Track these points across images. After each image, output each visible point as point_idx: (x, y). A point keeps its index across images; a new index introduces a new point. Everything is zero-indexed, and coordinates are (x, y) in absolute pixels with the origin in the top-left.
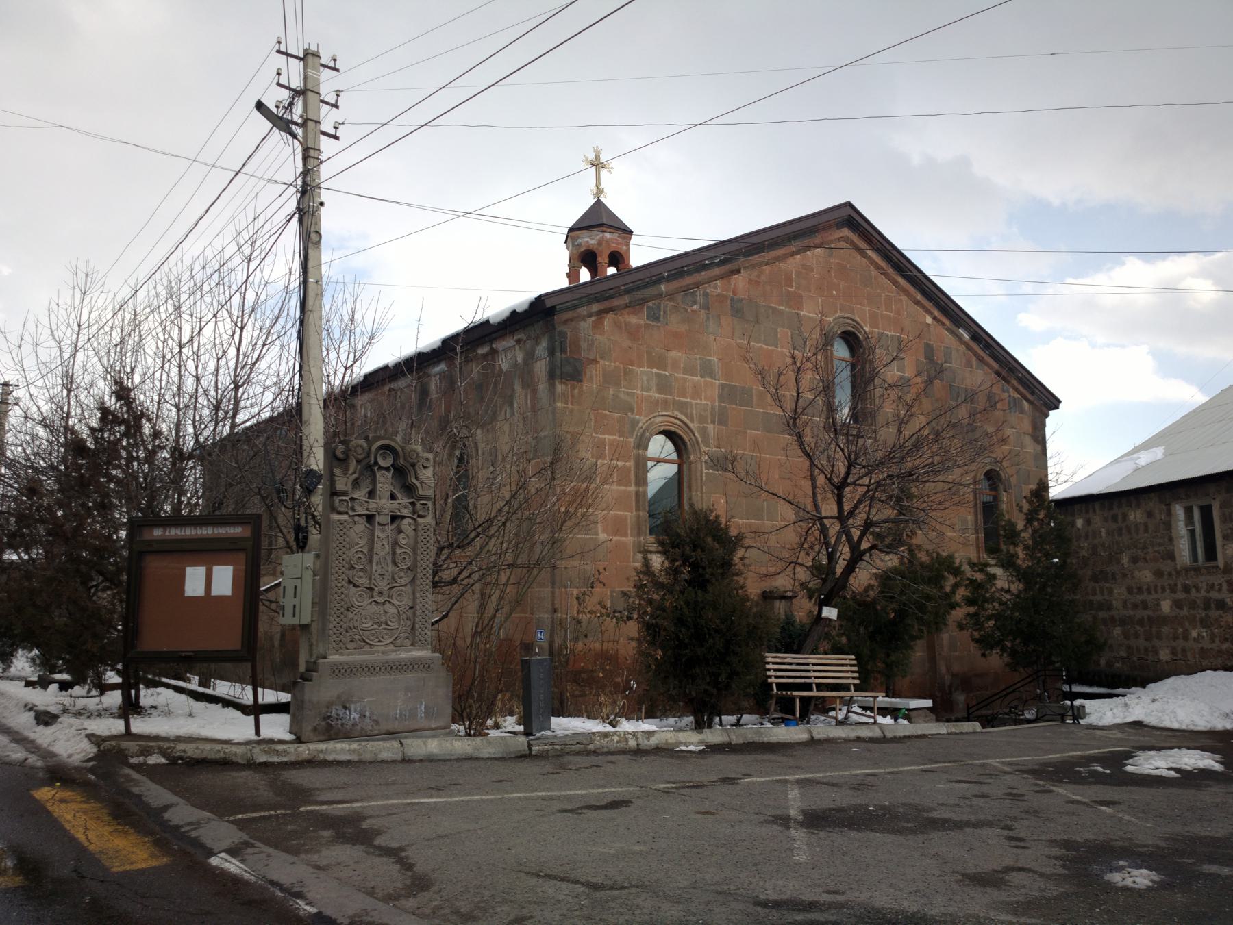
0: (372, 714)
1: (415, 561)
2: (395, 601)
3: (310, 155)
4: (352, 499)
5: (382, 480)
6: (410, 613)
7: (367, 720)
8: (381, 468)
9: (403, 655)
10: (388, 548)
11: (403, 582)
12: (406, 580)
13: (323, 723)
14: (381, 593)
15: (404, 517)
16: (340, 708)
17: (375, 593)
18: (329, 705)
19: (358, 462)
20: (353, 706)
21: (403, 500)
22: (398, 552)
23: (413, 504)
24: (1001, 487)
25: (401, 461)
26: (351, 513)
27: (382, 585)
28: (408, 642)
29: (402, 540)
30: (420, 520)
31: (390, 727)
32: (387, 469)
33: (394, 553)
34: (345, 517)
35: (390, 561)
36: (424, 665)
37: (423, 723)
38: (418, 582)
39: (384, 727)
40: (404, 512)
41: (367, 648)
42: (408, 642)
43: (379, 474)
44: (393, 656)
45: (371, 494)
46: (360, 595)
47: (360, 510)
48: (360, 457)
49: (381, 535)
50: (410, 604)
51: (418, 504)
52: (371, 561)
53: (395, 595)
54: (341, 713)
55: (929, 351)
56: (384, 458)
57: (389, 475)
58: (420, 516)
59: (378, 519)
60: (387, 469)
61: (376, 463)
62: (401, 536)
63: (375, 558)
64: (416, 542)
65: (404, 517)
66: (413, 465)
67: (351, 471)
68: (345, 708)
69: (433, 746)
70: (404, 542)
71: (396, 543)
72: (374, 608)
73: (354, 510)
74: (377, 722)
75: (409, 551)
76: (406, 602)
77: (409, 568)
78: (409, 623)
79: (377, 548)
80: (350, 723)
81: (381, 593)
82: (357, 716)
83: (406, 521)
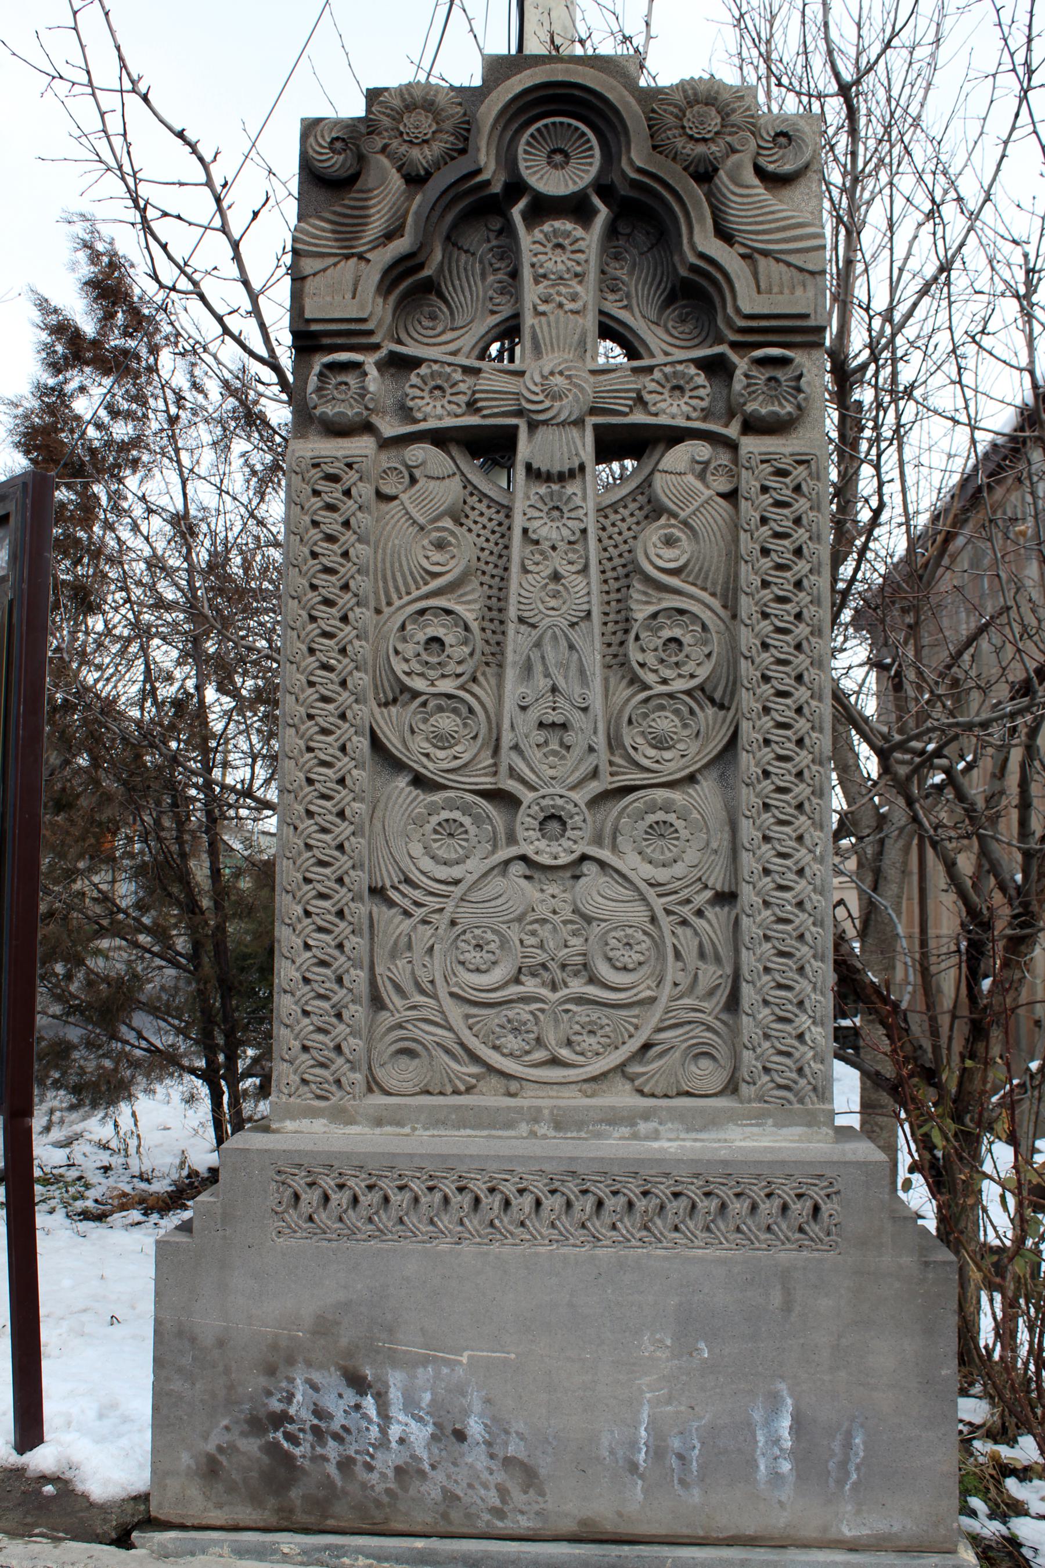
0: (498, 1428)
1: (733, 654)
2: (630, 862)
4: (400, 364)
5: (556, 262)
6: (714, 924)
7: (476, 1458)
8: (543, 208)
9: (672, 1143)
10: (586, 591)
11: (673, 765)
12: (689, 752)
13: (251, 1446)
14: (553, 820)
15: (674, 436)
16: (331, 1380)
17: (526, 820)
18: (276, 1363)
19: (415, 180)
20: (396, 1382)
22: (641, 613)
23: (716, 368)
25: (638, 155)
26: (390, 428)
27: (552, 777)
28: (707, 1075)
29: (654, 550)
30: (752, 445)
31: (602, 1508)
32: (576, 208)
33: (622, 623)
34: (362, 446)
35: (594, 657)
36: (800, 1206)
37: (787, 1508)
38: (748, 763)
39: (569, 1502)
40: (672, 411)
41: (490, 1098)
42: (707, 1075)
43: (529, 241)
44: (615, 1145)
46: (449, 830)
47: (439, 413)
48: (421, 157)
49: (546, 530)
50: (718, 880)
51: (741, 364)
53: (633, 830)
54: (338, 1403)
57: (590, 238)
58: (752, 426)
59: (525, 449)
60: (576, 208)
61: (516, 187)
62: (653, 533)
63: (517, 642)
64: (734, 557)
65: (674, 436)
66: (705, 174)
67: (376, 226)
68: (357, 1383)
70: (671, 557)
72: (517, 890)
73: (406, 413)
74: (529, 1476)
75: (705, 605)
76: (693, 860)
77: (703, 693)
78: (710, 974)
79: (524, 589)
80: (387, 1461)
81: (553, 820)
82: (420, 1434)
83: (678, 457)
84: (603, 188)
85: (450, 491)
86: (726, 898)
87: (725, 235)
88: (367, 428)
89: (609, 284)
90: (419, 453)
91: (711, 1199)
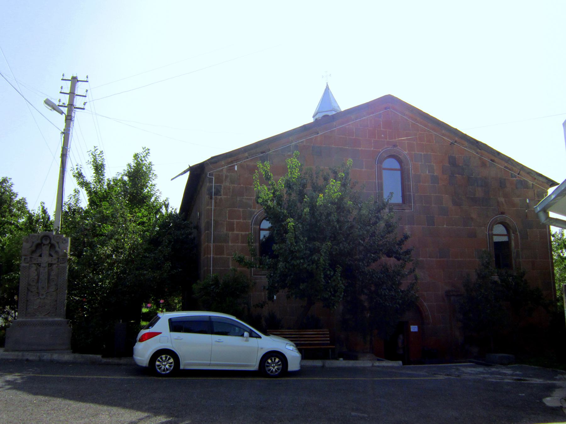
3: (69, 119)
8: (44, 245)
9: (50, 319)
11: (53, 290)
14: (42, 295)
21: (55, 256)
24: (511, 232)
30: (61, 265)
32: (48, 244)
40: (54, 262)
45: (40, 256)
47: (35, 262)
52: (38, 282)
55: (453, 162)
56: (46, 240)
60: (48, 244)
61: (42, 243)
63: (40, 281)
69: (56, 356)
71: (49, 275)
79: (41, 277)
83: (54, 266)
84: (50, 243)
85: (35, 268)
86: (56, 301)
87: (59, 247)
88: (28, 263)
89: (50, 250)
90: (33, 265)
91: (53, 323)
